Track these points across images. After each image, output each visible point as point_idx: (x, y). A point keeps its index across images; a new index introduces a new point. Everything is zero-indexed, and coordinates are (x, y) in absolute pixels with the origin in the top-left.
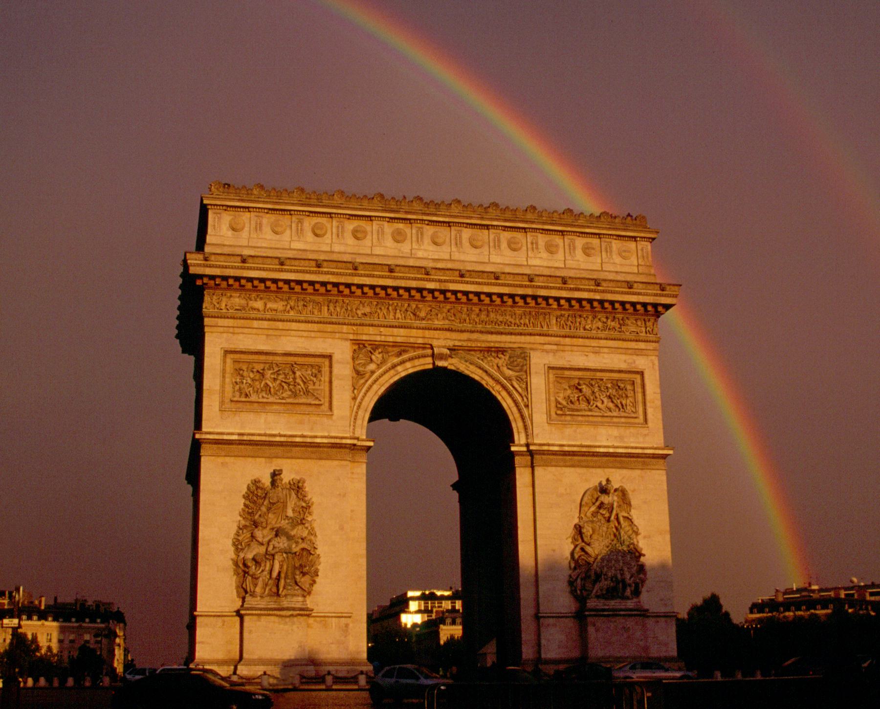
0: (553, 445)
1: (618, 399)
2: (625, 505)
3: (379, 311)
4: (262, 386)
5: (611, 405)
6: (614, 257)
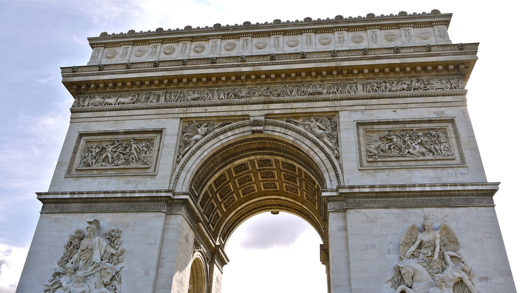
0: (364, 187)
1: (431, 145)
2: (452, 243)
3: (205, 95)
4: (103, 157)
5: (424, 150)
6: (414, 38)
